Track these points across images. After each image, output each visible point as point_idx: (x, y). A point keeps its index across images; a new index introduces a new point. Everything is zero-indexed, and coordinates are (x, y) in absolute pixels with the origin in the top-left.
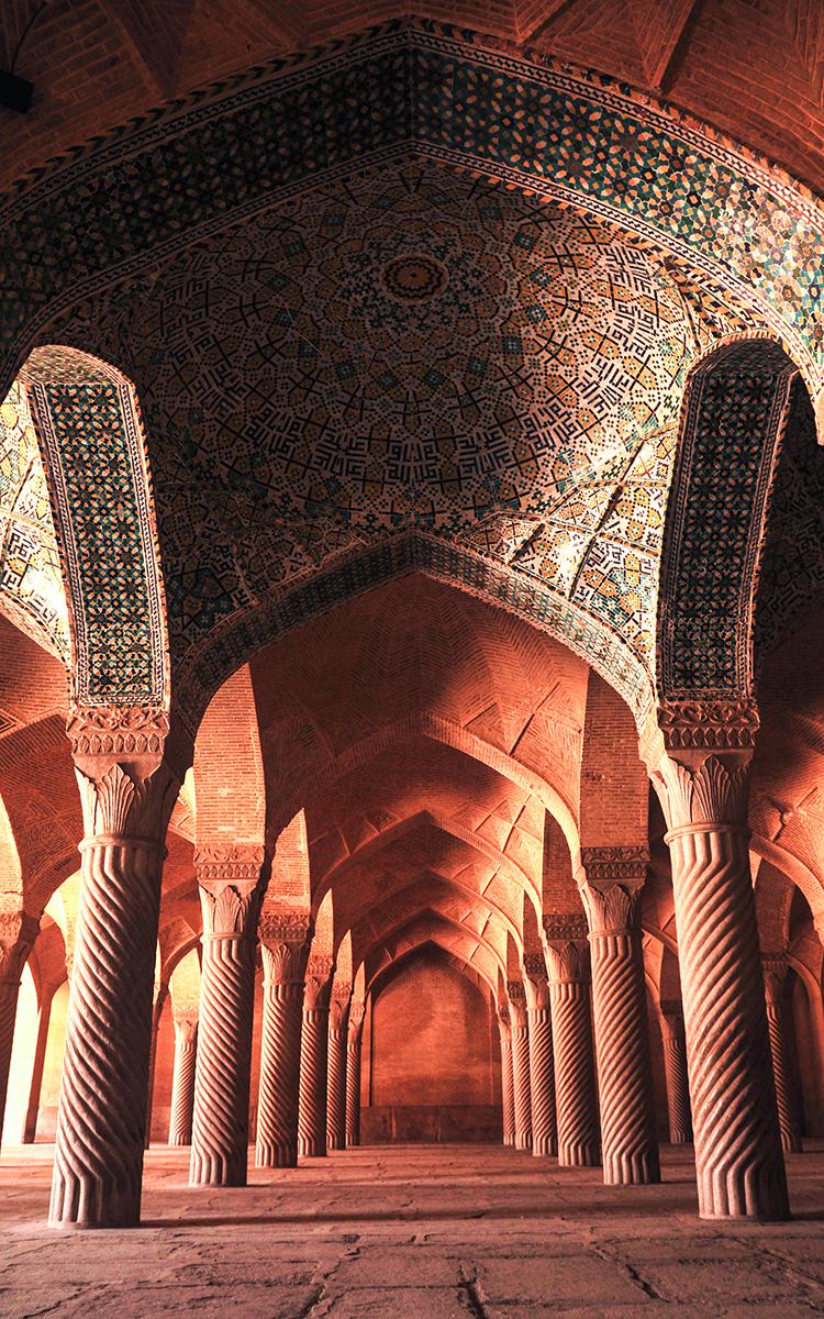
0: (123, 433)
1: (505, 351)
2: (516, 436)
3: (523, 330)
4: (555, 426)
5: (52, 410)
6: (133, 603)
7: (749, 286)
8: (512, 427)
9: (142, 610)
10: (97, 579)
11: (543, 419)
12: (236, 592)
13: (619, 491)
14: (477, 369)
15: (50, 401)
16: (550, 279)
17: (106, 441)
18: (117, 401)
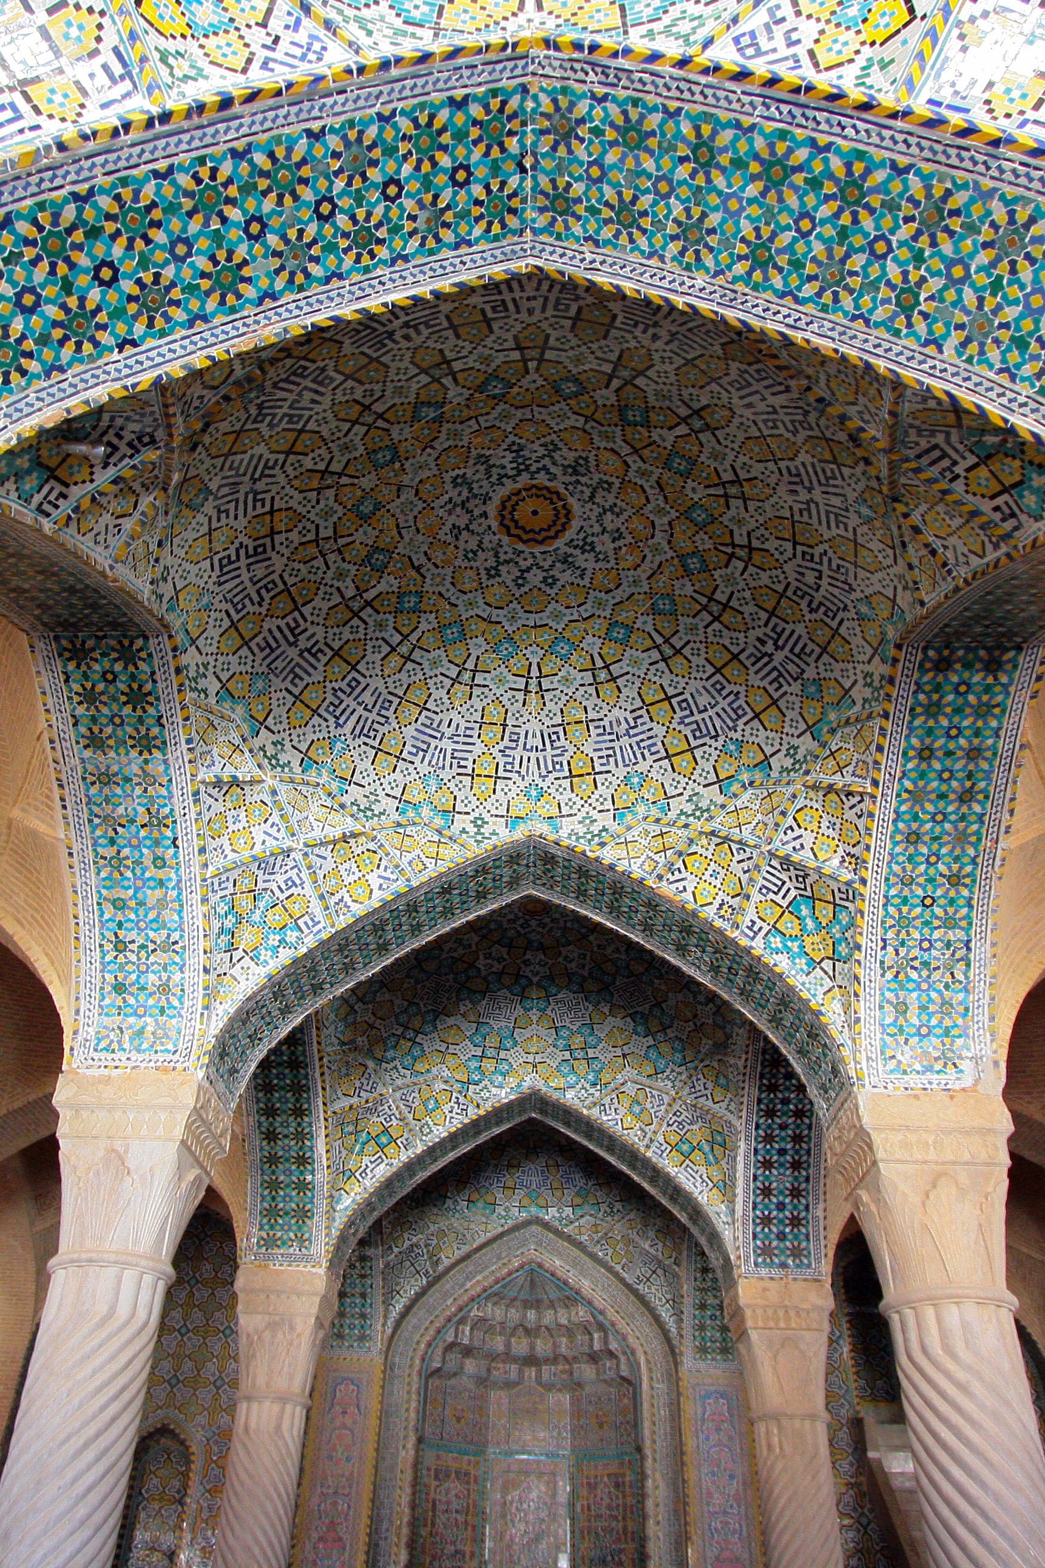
0: (431, 252)
1: (441, 628)
2: (330, 676)
3: (481, 640)
4: (366, 714)
5: (476, 98)
6: (43, 340)
7: (879, 972)
8: (339, 667)
9: (33, 366)
10: (78, 236)
11: (367, 698)
12: (59, 488)
13: (354, 835)
14: (406, 605)
15: (494, 93)
16: (565, 659)
17: (413, 218)
18: (496, 238)
